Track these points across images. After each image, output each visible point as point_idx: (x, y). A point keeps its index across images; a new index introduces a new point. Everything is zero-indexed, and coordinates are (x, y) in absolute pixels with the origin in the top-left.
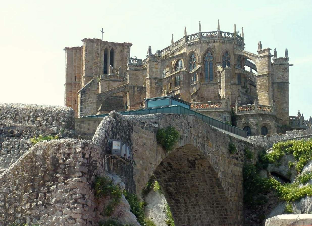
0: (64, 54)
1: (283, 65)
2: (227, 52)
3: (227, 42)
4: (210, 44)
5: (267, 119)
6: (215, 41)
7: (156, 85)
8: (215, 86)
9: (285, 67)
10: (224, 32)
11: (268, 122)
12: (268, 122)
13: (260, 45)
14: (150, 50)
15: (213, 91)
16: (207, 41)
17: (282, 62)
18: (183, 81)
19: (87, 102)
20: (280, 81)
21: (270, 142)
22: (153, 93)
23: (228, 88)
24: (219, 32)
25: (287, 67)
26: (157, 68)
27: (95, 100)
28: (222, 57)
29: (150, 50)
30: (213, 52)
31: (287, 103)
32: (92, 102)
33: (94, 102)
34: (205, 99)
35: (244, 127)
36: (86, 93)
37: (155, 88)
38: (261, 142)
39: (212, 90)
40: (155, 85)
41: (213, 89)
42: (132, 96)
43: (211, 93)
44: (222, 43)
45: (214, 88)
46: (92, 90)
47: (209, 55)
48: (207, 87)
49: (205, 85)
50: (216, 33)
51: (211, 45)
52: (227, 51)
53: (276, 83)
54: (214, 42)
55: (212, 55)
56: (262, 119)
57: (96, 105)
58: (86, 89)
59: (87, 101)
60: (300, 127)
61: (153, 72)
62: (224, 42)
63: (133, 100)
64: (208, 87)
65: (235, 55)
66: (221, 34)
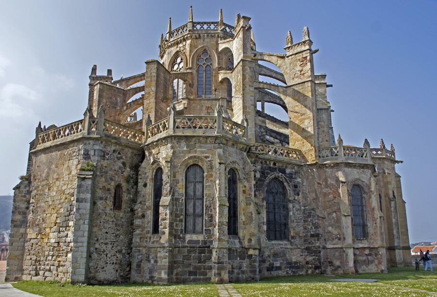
5: (200, 147)
9: (304, 56)
10: (198, 23)
11: (203, 152)
12: (203, 152)
14: (94, 69)
29: (94, 69)
35: (155, 171)
52: (205, 50)
55: (182, 60)
56: (185, 149)
60: (339, 159)
62: (200, 36)
65: (219, 54)
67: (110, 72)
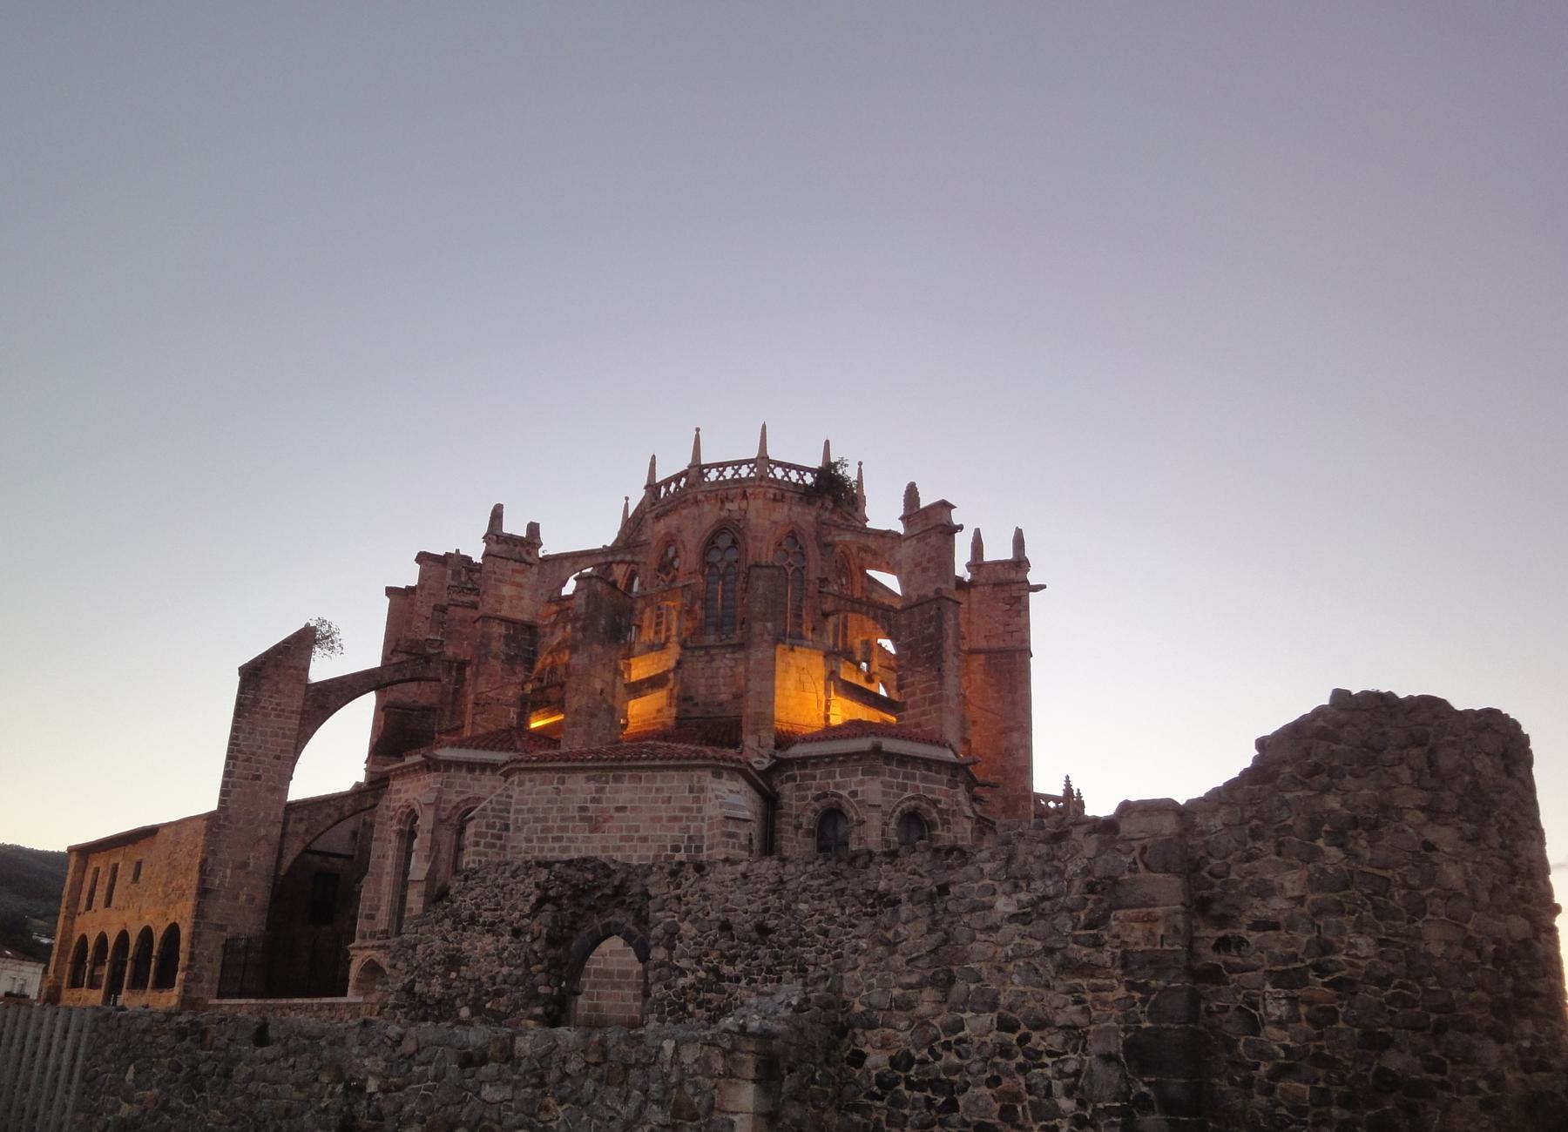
0: (386, 602)
1: (1006, 588)
2: (793, 535)
3: (792, 498)
4: (728, 506)
6: (749, 491)
7: (507, 645)
8: (737, 656)
10: (780, 464)
13: (912, 494)
14: (497, 515)
15: (730, 674)
16: (720, 492)
17: (1002, 575)
18: (582, 617)
19: (264, 708)
20: (996, 644)
21: (881, 896)
22: (491, 675)
23: (765, 645)
24: (763, 460)
25: (1022, 593)
26: (519, 585)
27: (297, 703)
28: (772, 548)
29: (497, 515)
30: (739, 532)
31: (1025, 728)
32: (283, 710)
33: (292, 712)
34: (696, 705)
36: (264, 678)
37: (503, 657)
38: (821, 898)
39: (728, 671)
40: (503, 648)
41: (731, 668)
42: (450, 699)
43: (722, 681)
44: (775, 500)
45: (731, 664)
46: (290, 667)
47: (725, 541)
48: (706, 658)
49: (702, 652)
50: (751, 465)
51: (733, 506)
52: (792, 531)
53: (979, 652)
54: (745, 496)
57: (297, 722)
58: (264, 663)
59: (262, 704)
61: (504, 597)
62: (783, 496)
63: (453, 713)
64: (712, 660)
66: (772, 470)
67: (533, 529)
